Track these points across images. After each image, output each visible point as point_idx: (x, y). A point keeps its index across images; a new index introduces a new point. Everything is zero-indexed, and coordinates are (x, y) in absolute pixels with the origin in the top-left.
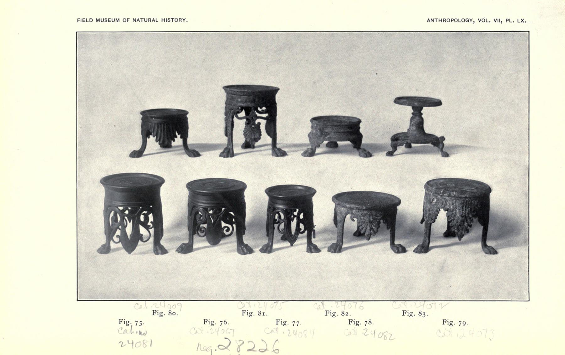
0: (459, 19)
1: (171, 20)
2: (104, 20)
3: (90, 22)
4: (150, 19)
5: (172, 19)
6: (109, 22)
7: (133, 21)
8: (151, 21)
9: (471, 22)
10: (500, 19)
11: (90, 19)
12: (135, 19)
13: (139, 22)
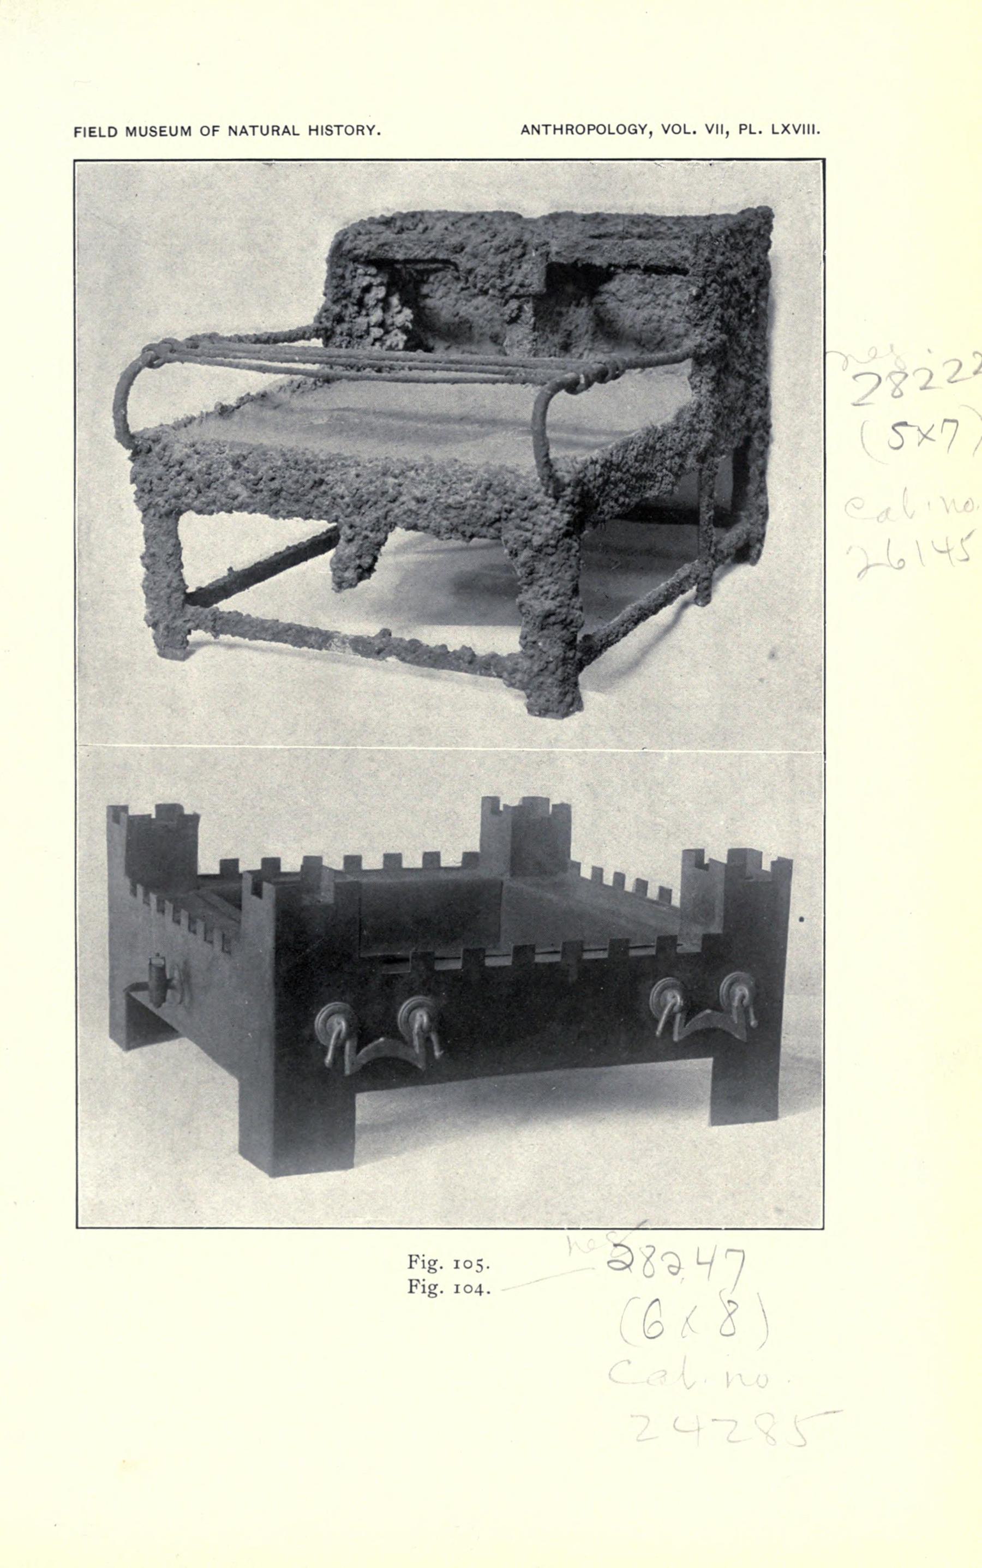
0: (609, 125)
1: (335, 130)
4: (276, 128)
5: (338, 126)
6: (161, 135)
7: (230, 135)
8: (278, 134)
11: (110, 128)
12: (234, 129)
13: (245, 134)
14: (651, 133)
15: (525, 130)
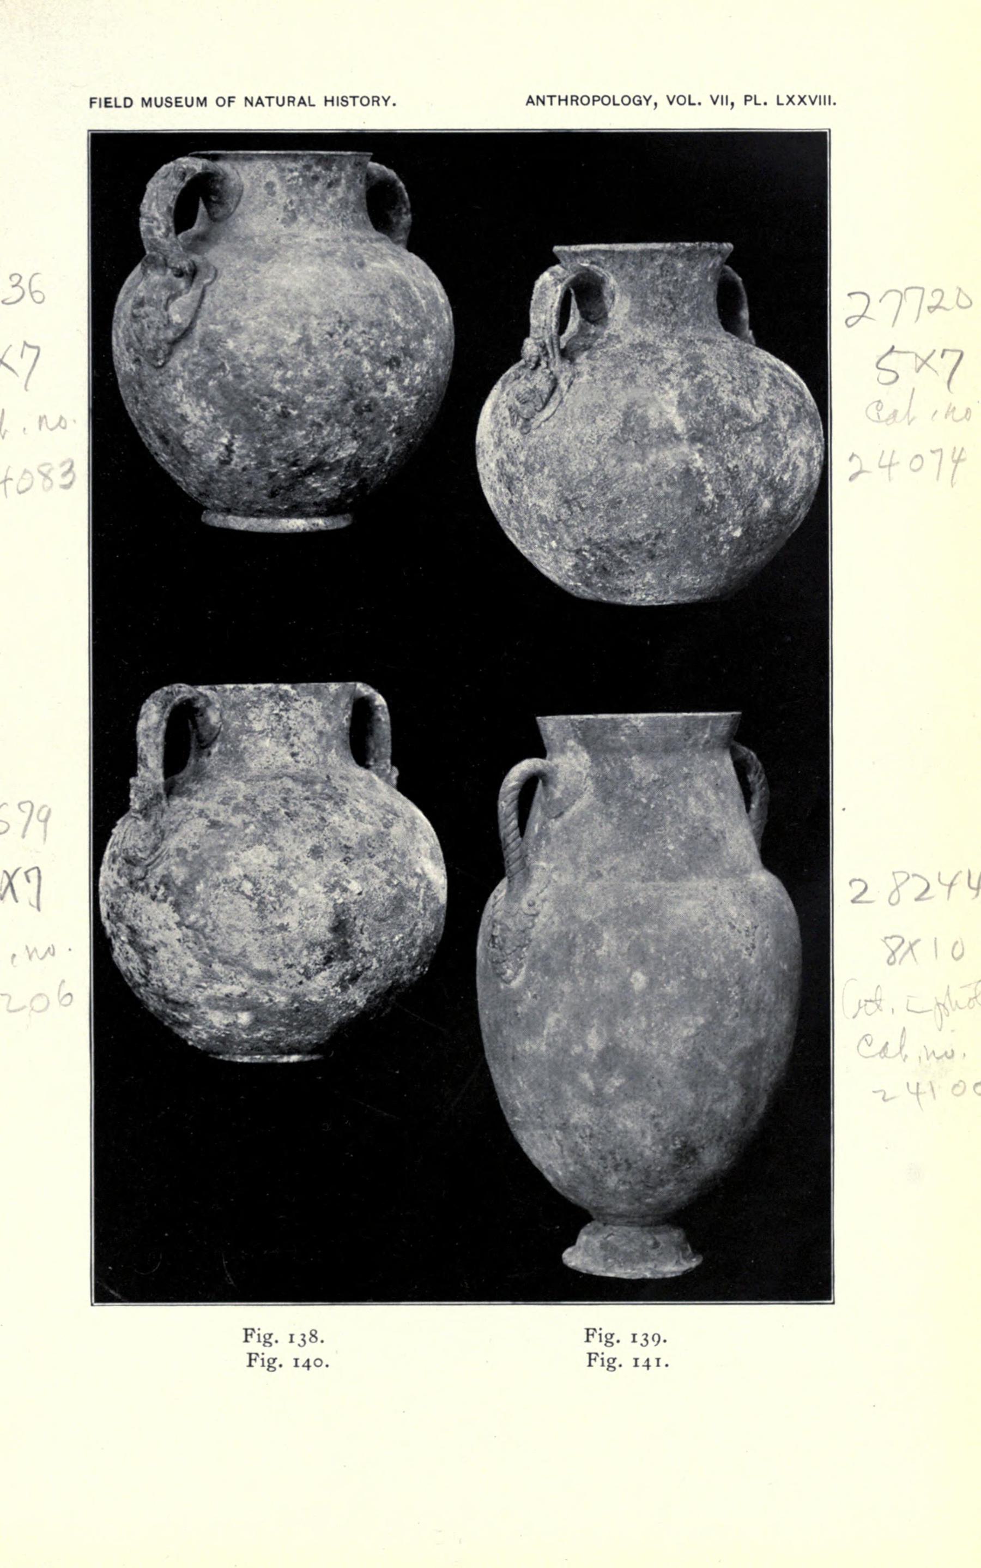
1: (350, 100)
5: (354, 97)
11: (125, 99)
14: (656, 104)
15: (530, 101)
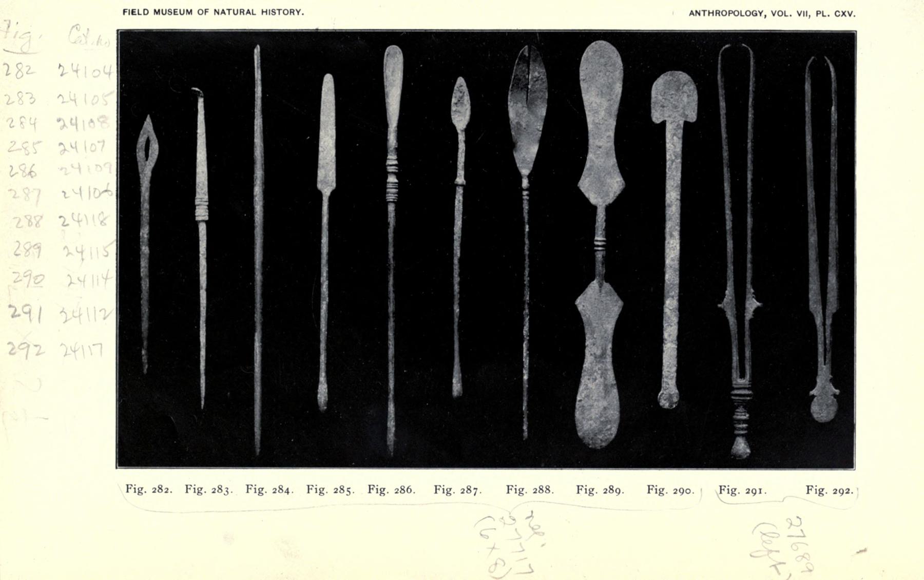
2: (167, 12)
3: (144, 14)
4: (242, 11)
5: (279, 10)
6: (174, 14)
7: (215, 14)
8: (244, 14)
9: (761, 15)
10: (807, 12)
11: (144, 10)
12: (217, 11)
